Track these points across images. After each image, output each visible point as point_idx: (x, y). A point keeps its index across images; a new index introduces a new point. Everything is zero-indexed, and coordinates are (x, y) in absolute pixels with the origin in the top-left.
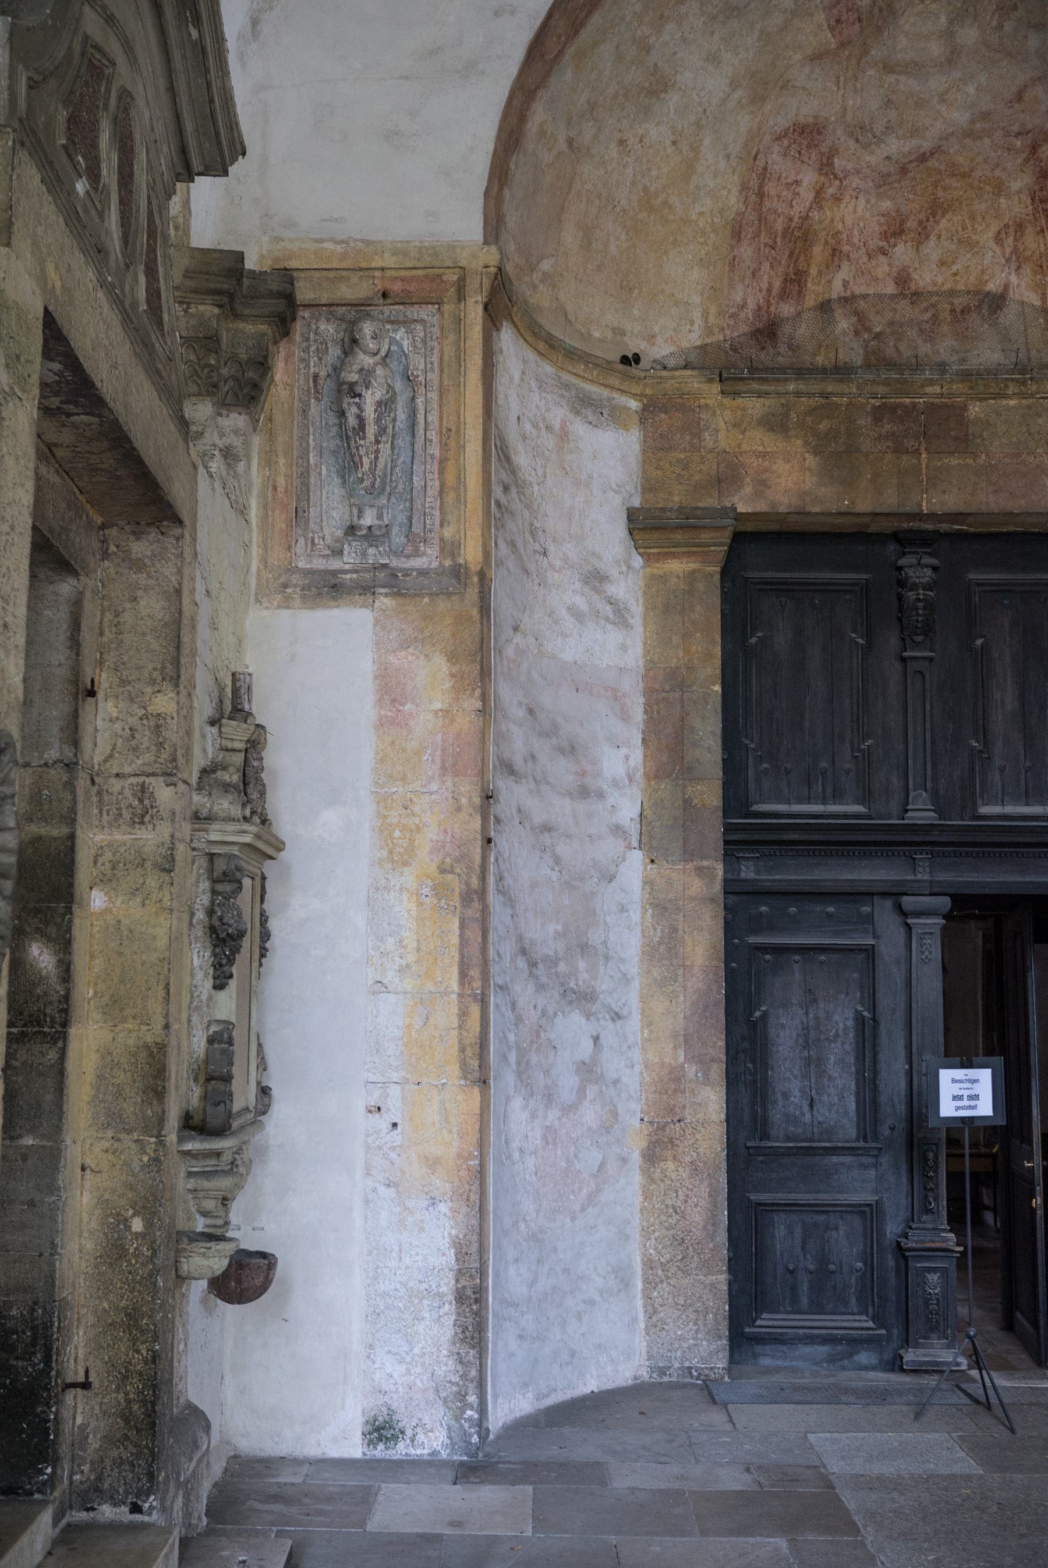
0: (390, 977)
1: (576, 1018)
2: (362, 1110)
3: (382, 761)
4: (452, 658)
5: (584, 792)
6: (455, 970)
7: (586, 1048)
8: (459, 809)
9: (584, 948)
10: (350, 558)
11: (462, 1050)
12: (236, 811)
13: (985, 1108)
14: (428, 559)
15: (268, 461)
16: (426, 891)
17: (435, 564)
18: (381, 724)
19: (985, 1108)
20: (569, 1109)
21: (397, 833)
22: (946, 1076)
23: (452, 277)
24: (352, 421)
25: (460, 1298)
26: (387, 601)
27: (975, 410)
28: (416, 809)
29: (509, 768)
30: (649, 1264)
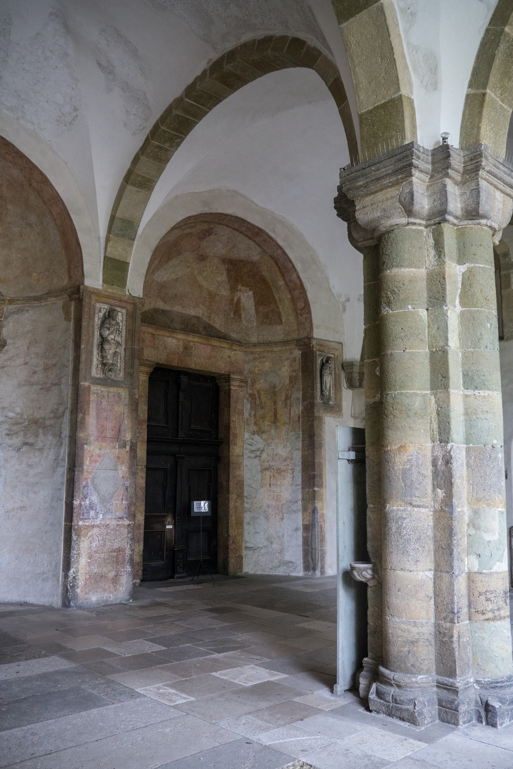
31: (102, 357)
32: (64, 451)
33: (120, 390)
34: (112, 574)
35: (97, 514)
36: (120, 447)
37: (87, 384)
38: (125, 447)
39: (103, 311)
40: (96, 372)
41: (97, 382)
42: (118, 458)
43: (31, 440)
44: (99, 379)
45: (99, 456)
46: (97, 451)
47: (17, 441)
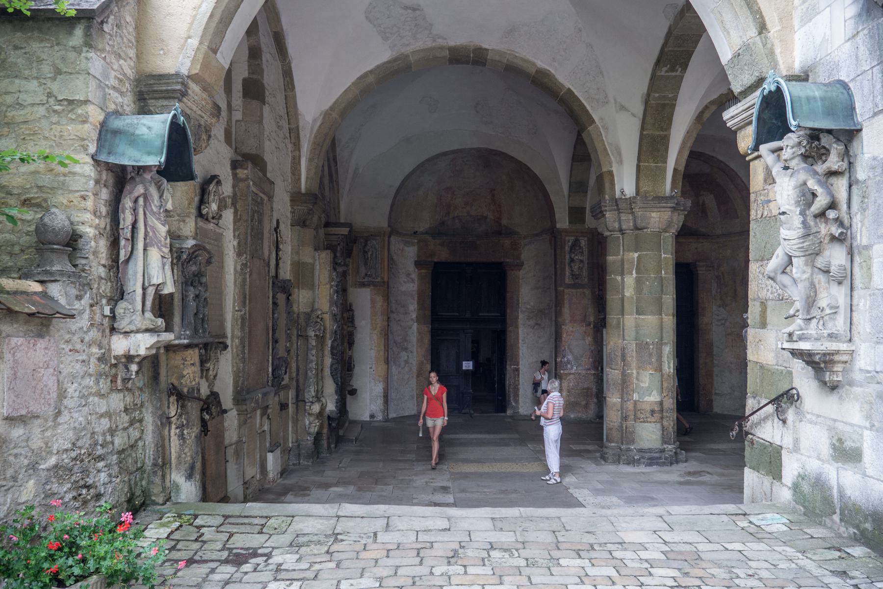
1: (404, 353)
5: (406, 313)
7: (406, 358)
9: (406, 341)
10: (366, 280)
13: (471, 368)
14: (379, 280)
18: (372, 307)
19: (471, 368)
20: (403, 368)
22: (464, 362)
25: (384, 396)
27: (478, 242)
29: (392, 312)
30: (417, 395)
31: (572, 271)
32: (553, 329)
33: (585, 290)
34: (583, 403)
35: (572, 367)
36: (587, 326)
37: (562, 289)
38: (589, 325)
39: (571, 242)
40: (568, 281)
41: (569, 286)
42: (585, 332)
43: (539, 322)
44: (571, 284)
45: (572, 332)
46: (571, 329)
47: (532, 322)
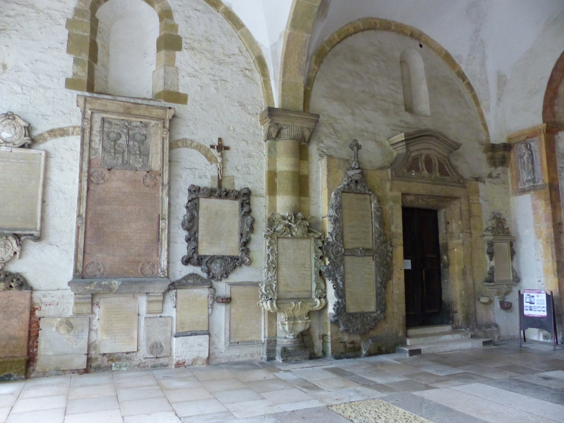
0: (540, 258)
2: (537, 281)
3: (535, 220)
4: (545, 200)
6: (551, 257)
8: (549, 227)
11: (553, 271)
12: (490, 234)
15: (511, 171)
16: (545, 242)
17: (542, 183)
18: (534, 214)
21: (538, 233)
23: (538, 131)
24: (523, 162)
26: (533, 192)
28: (541, 228)
